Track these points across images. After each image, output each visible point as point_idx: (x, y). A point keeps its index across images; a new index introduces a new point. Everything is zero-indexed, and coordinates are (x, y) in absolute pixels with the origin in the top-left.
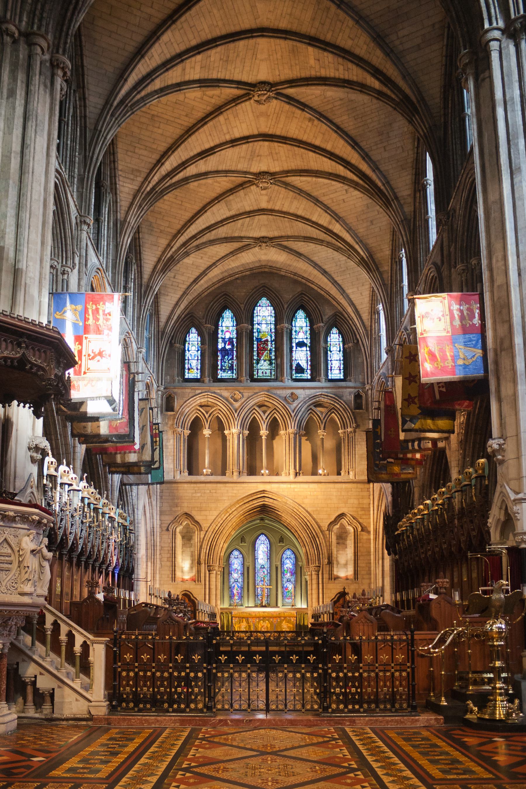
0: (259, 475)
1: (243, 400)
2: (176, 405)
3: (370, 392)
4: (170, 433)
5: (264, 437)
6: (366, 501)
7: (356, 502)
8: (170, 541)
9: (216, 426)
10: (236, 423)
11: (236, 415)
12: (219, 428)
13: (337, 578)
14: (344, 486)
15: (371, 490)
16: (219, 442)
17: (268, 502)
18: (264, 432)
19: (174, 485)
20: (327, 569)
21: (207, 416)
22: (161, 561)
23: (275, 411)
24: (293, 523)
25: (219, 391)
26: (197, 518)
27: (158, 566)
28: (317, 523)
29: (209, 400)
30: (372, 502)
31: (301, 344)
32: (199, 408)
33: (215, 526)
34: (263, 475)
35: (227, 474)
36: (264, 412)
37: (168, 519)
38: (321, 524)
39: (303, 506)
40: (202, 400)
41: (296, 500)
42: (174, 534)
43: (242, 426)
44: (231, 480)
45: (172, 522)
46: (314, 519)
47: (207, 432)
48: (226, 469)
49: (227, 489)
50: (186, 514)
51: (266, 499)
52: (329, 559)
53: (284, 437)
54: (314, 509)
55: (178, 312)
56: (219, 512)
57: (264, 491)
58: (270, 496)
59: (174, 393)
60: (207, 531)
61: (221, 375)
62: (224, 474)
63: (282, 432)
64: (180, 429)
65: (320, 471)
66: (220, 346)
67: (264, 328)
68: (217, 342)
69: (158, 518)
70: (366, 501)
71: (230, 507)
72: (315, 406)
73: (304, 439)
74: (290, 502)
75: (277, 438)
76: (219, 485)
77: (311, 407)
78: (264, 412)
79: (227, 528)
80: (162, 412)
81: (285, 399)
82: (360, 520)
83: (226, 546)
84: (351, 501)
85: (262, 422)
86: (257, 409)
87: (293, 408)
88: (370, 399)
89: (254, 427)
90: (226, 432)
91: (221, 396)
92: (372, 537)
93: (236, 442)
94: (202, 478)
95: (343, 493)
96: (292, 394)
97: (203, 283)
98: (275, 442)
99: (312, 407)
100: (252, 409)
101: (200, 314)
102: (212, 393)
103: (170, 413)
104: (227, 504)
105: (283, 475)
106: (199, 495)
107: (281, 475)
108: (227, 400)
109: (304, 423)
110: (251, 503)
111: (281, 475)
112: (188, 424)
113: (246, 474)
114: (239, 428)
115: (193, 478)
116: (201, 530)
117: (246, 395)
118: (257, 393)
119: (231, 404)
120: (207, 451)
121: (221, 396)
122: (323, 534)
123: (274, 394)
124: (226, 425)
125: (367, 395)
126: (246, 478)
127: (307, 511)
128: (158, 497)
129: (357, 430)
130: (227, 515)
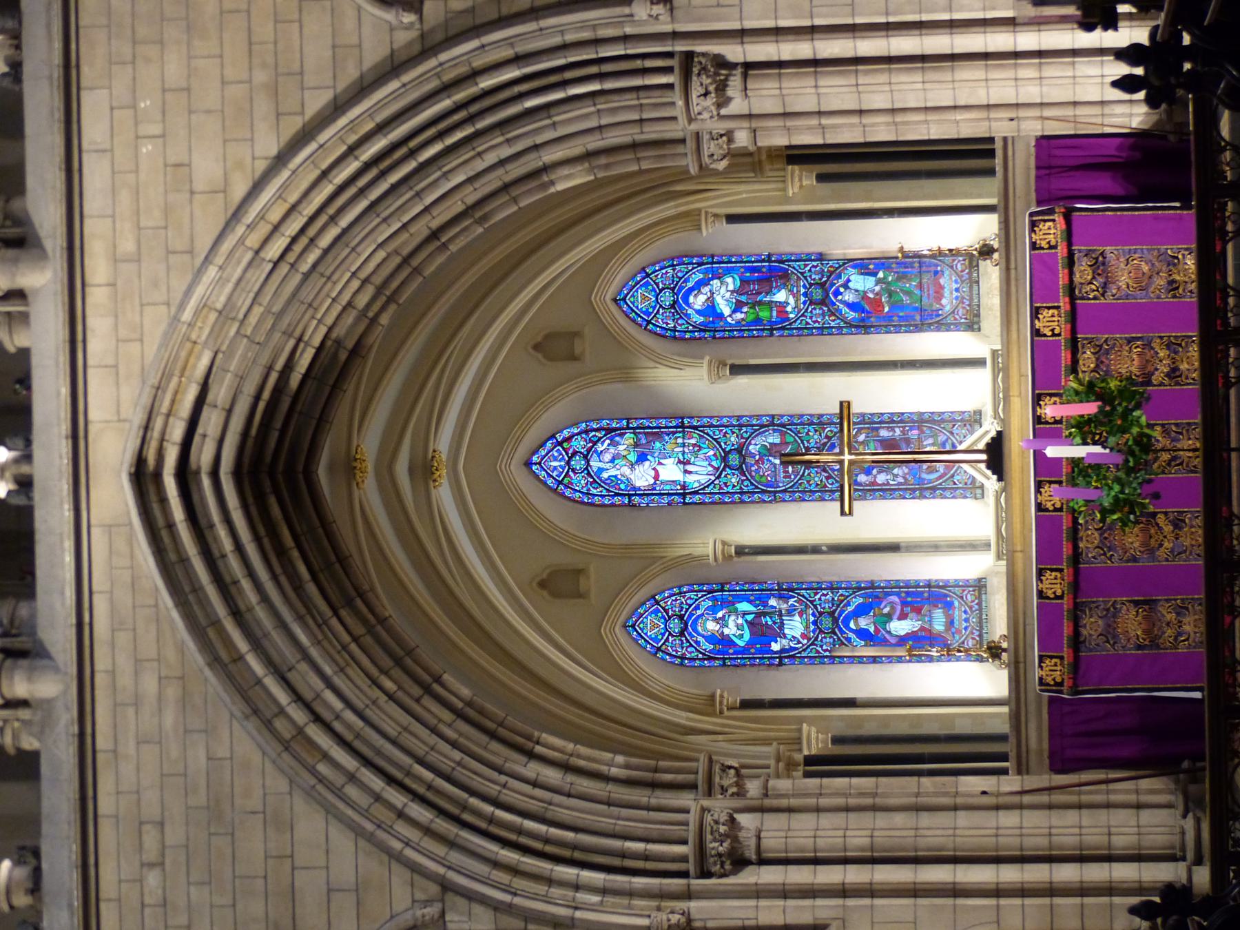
28: (362, 89)
38: (374, 53)
39: (240, 189)
41: (204, 244)
44: (66, 718)
46: (338, 107)
49: (128, 747)
51: (203, 456)
54: (263, 106)
58: (177, 432)
60: (446, 887)
76: (106, 804)
107: (24, 354)
111: (24, 354)
113: (23, 610)
127: (281, 159)
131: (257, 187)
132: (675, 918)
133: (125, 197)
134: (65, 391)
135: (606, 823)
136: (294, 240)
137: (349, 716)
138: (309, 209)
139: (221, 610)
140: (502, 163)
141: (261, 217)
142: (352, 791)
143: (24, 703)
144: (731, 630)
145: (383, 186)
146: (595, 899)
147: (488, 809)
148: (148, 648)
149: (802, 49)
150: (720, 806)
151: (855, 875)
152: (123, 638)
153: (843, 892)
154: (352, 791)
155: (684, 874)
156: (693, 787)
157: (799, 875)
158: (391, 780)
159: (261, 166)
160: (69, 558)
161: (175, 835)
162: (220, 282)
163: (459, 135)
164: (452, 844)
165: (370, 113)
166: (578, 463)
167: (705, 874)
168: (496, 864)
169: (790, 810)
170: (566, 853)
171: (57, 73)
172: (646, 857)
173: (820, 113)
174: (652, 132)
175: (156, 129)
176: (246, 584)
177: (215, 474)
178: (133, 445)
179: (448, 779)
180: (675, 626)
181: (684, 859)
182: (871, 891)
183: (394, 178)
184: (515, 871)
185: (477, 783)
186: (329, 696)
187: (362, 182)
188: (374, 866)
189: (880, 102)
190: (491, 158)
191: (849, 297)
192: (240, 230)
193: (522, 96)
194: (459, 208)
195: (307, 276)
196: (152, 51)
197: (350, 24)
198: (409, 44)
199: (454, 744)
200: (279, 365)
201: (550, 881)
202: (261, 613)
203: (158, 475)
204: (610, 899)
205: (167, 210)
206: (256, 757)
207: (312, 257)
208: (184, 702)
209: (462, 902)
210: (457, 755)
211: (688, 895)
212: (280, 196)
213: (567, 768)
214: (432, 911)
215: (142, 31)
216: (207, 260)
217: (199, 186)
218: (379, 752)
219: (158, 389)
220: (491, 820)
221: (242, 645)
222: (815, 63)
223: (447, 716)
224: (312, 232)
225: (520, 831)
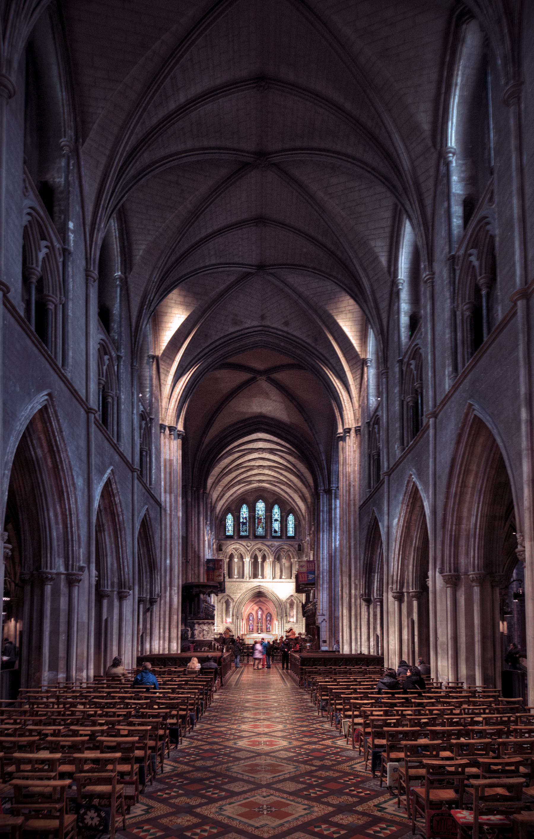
2: (224, 549)
13: (289, 622)
16: (241, 563)
17: (261, 590)
18: (260, 560)
20: (285, 618)
26: (232, 597)
31: (276, 520)
43: (251, 558)
47: (236, 560)
55: (224, 508)
61: (242, 534)
62: (243, 578)
65: (283, 577)
66: (241, 520)
67: (260, 513)
68: (240, 519)
89: (255, 558)
94: (234, 580)
97: (235, 495)
100: (255, 550)
101: (233, 508)
104: (244, 591)
112: (228, 556)
115: (231, 580)
126: (252, 580)
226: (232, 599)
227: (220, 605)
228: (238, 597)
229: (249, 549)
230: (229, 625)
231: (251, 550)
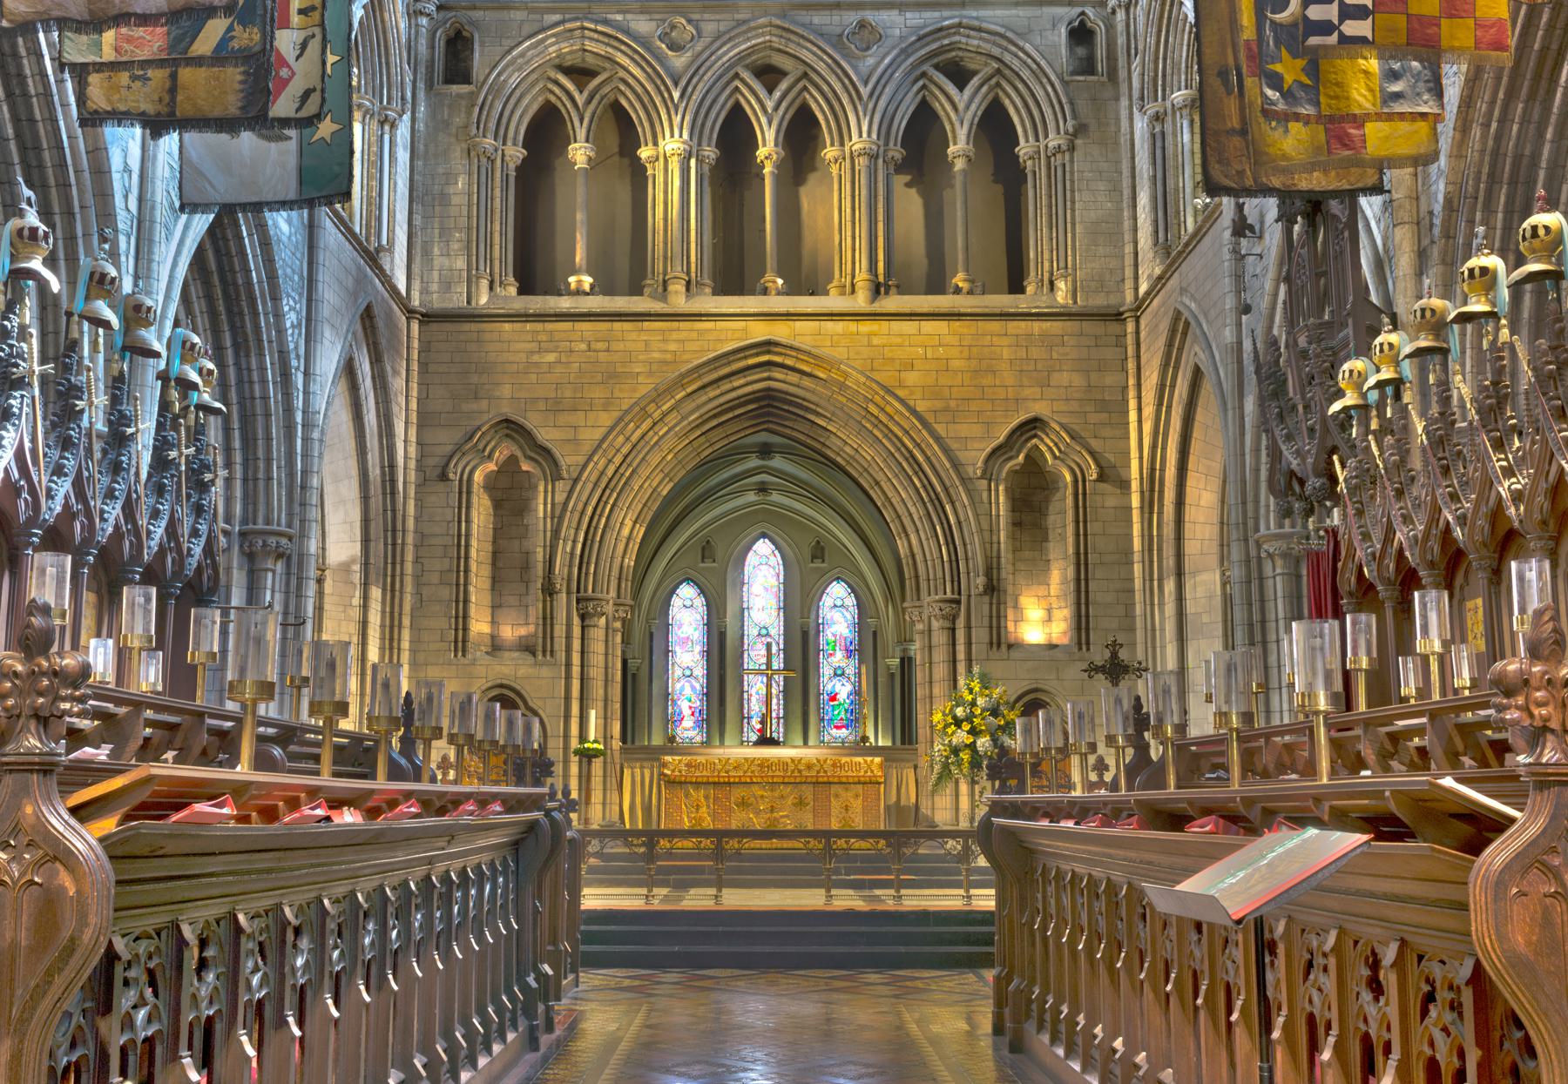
0: (752, 293)
1: (699, 48)
3: (1120, 15)
4: (457, 153)
5: (768, 170)
6: (1109, 379)
7: (1078, 380)
8: (450, 514)
9: (613, 141)
10: (677, 120)
11: (676, 95)
12: (621, 146)
14: (1037, 327)
15: (1130, 340)
16: (624, 194)
17: (782, 381)
19: (466, 327)
20: (981, 608)
21: (580, 99)
22: (417, 578)
23: (804, 82)
24: (868, 452)
25: (619, 17)
26: (544, 435)
27: (408, 599)
28: (946, 451)
29: (590, 45)
30: (1132, 381)
32: (553, 74)
33: (603, 462)
34: (765, 292)
35: (647, 290)
36: (770, 91)
37: (445, 439)
38: (963, 456)
39: (900, 393)
40: (566, 48)
41: (876, 376)
42: (466, 489)
43: (697, 130)
44: (657, 307)
45: (458, 448)
46: (938, 439)
47: (579, 153)
48: (644, 277)
50: (507, 421)
52: (988, 573)
53: (834, 170)
54: (939, 405)
56: (617, 414)
57: (768, 345)
58: (789, 362)
59: (471, 23)
60: (576, 481)
63: (829, 152)
64: (489, 141)
65: (959, 279)
69: (413, 437)
70: (1109, 379)
71: (658, 396)
72: (937, 67)
73: (900, 180)
74: (855, 380)
75: (813, 178)
76: (617, 325)
77: (925, 67)
78: (770, 91)
79: (645, 472)
80: (430, 86)
81: (838, 41)
82: (1095, 444)
83: (640, 532)
84: (1063, 378)
85: (764, 120)
86: (746, 75)
87: (864, 69)
88: (1121, 40)
90: (645, 153)
91: (627, 32)
92: (1135, 501)
93: (677, 183)
94: (564, 303)
95: (1035, 353)
96: (862, 25)
98: (804, 192)
99: (926, 67)
102: (596, 22)
103: (456, 89)
104: (645, 387)
105: (833, 292)
106: (551, 357)
107: (826, 293)
108: (645, 42)
109: (901, 123)
110: (726, 386)
112: (519, 125)
113: (708, 290)
114: (686, 135)
115: (536, 303)
116: (556, 476)
117: (709, 28)
118: (745, 22)
119: (661, 59)
120: (580, 217)
121: (627, 32)
122: (969, 492)
123: (803, 25)
124: (643, 129)
125: (1110, 27)
127: (914, 412)
128: (415, 366)
129: (1078, 142)
130: (644, 427)
131: (902, 401)
132: (558, 586)
133: (898, 340)
134: (809, 310)
135: (603, 556)
136: (877, 418)
137: (656, 438)
138: (891, 425)
139: (706, 380)
140: (910, 515)
141: (888, 403)
142: (621, 439)
143: (665, 289)
144: (685, 628)
145: (901, 460)
146: (568, 550)
147: (611, 502)
148: (690, 346)
149: (961, 656)
150: (609, 609)
151: (576, 670)
152: (694, 335)
153: (568, 665)
154: (621, 439)
155: (578, 591)
156: (619, 597)
157: (576, 645)
158: (626, 457)
159: (911, 403)
160: (731, 311)
161: (602, 356)
162: (858, 383)
163: (924, 495)
164: (596, 484)
165: (935, 454)
166: (764, 560)
167: (578, 601)
168: (586, 504)
169: (607, 641)
170: (590, 537)
171: (956, 311)
172: (587, 574)
173: (931, 663)
174: (924, 585)
175: (929, 356)
176: (718, 392)
177: (769, 379)
178: (784, 341)
179: (625, 483)
180: (688, 603)
181: (586, 591)
182: (568, 677)
183: (905, 464)
184: (583, 513)
185: (624, 496)
186: (666, 429)
187: (903, 449)
188: (587, 448)
189: (936, 691)
190: (913, 510)
191: (838, 688)
192: (882, 393)
193: (942, 524)
194: (890, 495)
195: (860, 423)
196: (966, 354)
197: (977, 446)
198: (967, 473)
199: (641, 487)
200: (819, 410)
201: (577, 529)
202: (704, 398)
203: (769, 352)
204: (568, 556)
205: (892, 359)
206: (638, 395)
207: (868, 425)
208: (665, 362)
209: (568, 488)
210: (636, 488)
211: (569, 593)
212: (897, 411)
213: (629, 539)
214: (565, 474)
215: (975, 350)
216: (868, 377)
217: (903, 374)
218: (639, 452)
219: (809, 353)
220: (606, 503)
221: (689, 390)
222: (954, 661)
223: (654, 484)
224: (880, 426)
225: (600, 516)
226: (544, 453)
227: (443, 500)
228: (592, 435)
229: (679, 61)
230: (514, 669)
231: (697, 70)
